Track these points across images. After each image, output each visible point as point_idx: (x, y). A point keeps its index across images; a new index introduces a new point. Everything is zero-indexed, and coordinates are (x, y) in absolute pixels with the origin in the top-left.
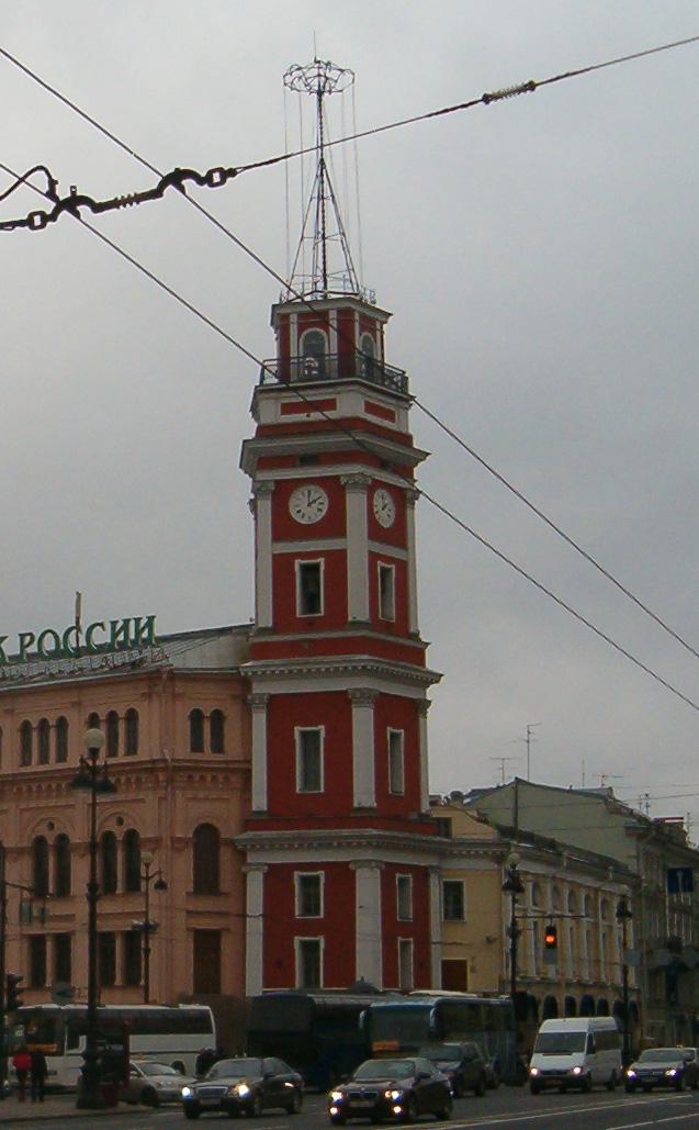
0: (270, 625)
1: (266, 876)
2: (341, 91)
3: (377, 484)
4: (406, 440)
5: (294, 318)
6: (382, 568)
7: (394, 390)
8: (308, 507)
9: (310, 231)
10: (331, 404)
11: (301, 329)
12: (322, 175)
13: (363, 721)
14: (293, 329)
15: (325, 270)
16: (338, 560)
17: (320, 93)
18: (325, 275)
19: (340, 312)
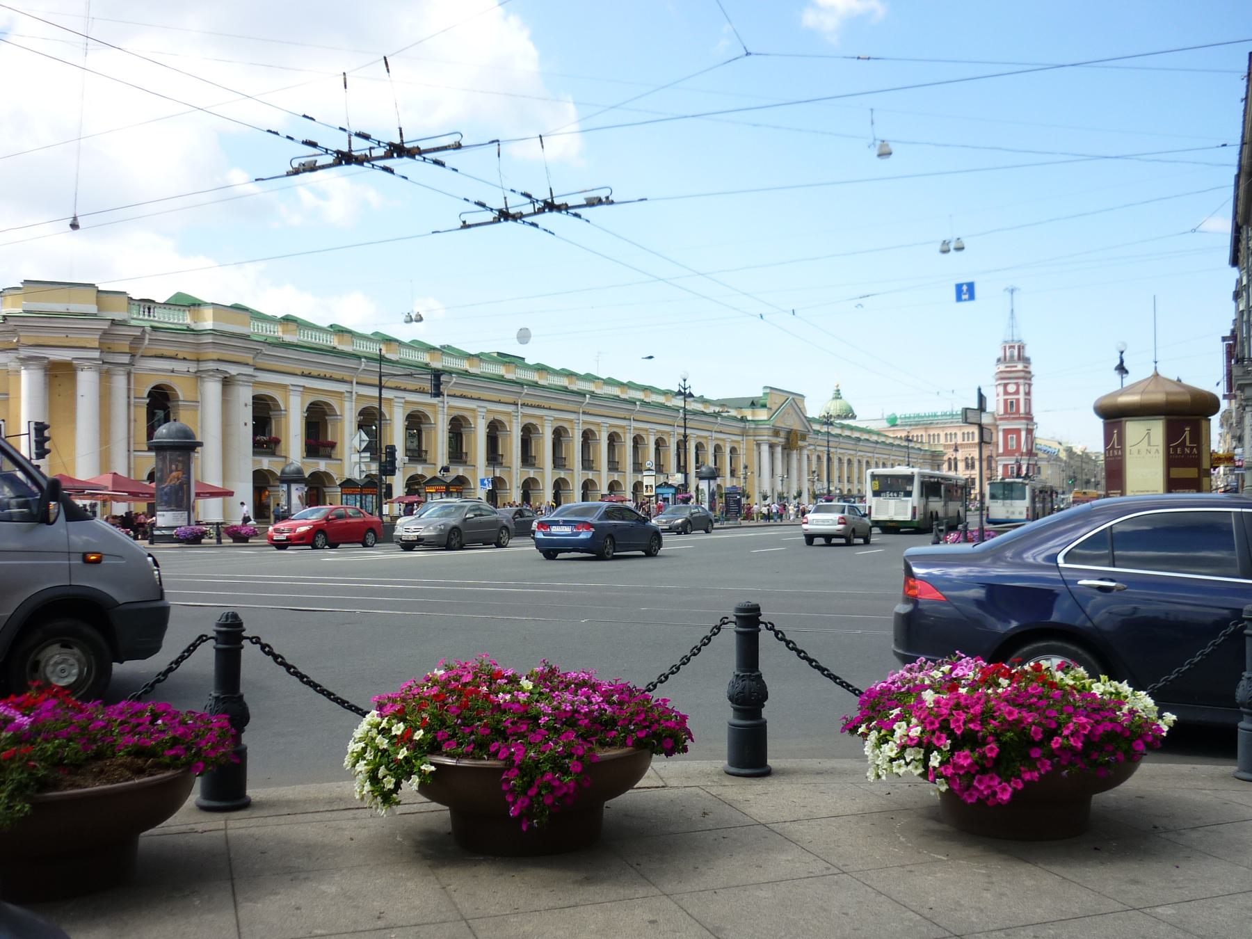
3: (1026, 383)
4: (1029, 372)
7: (1027, 361)
8: (1011, 388)
10: (1016, 366)
11: (1009, 349)
13: (1023, 434)
14: (1007, 349)
16: (1018, 400)
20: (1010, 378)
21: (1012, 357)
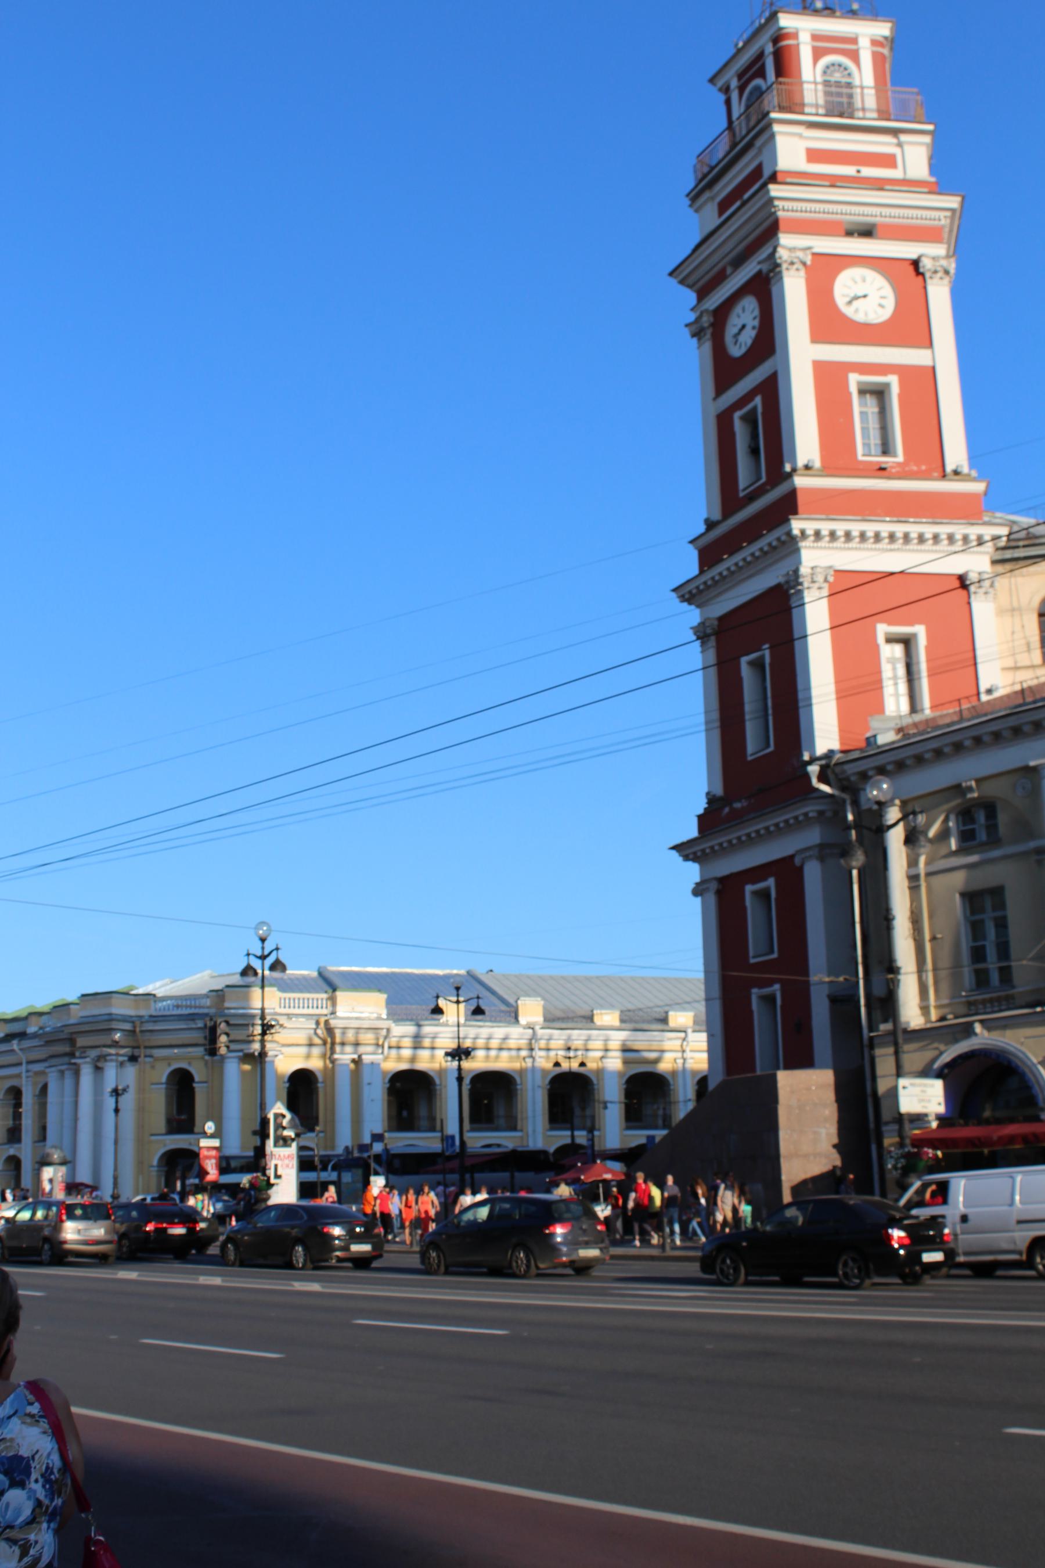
0: (717, 516)
1: (719, 893)
11: (742, 89)
14: (735, 96)
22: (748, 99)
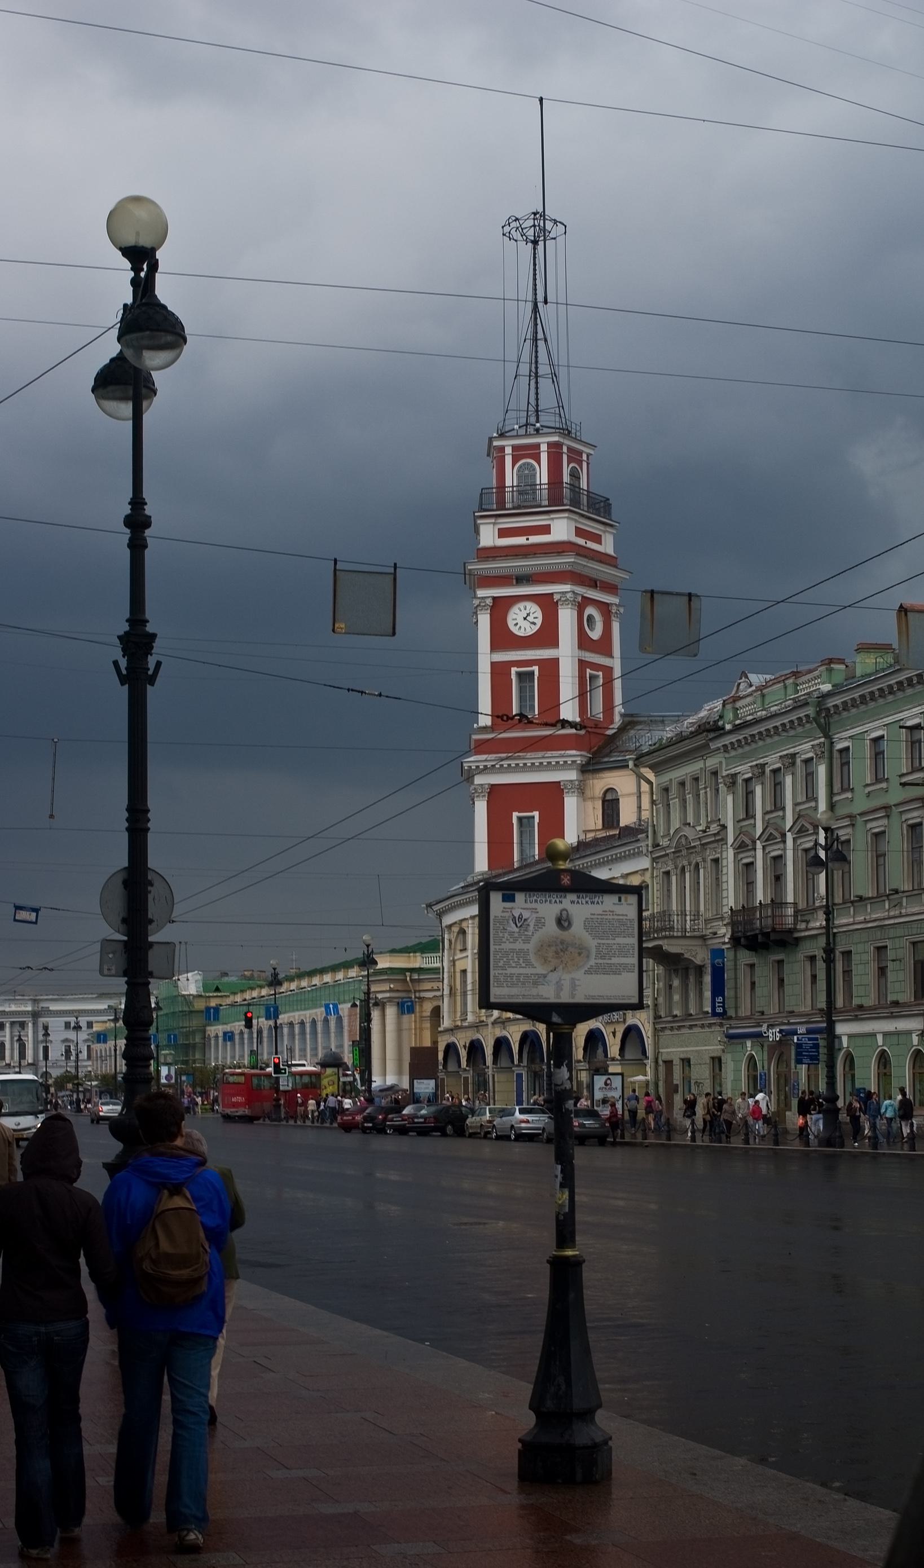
2: (555, 239)
5: (508, 450)
6: (590, 674)
9: (524, 369)
12: (536, 319)
14: (508, 460)
15: (537, 405)
16: (551, 667)
17: (535, 243)
18: (537, 411)
19: (550, 445)
20: (521, 580)
21: (527, 485)
22: (520, 467)
